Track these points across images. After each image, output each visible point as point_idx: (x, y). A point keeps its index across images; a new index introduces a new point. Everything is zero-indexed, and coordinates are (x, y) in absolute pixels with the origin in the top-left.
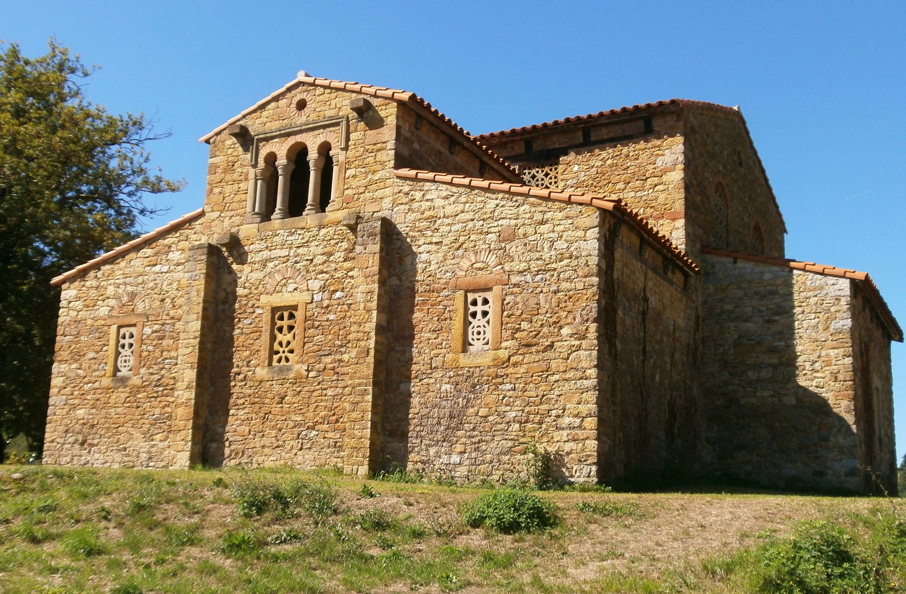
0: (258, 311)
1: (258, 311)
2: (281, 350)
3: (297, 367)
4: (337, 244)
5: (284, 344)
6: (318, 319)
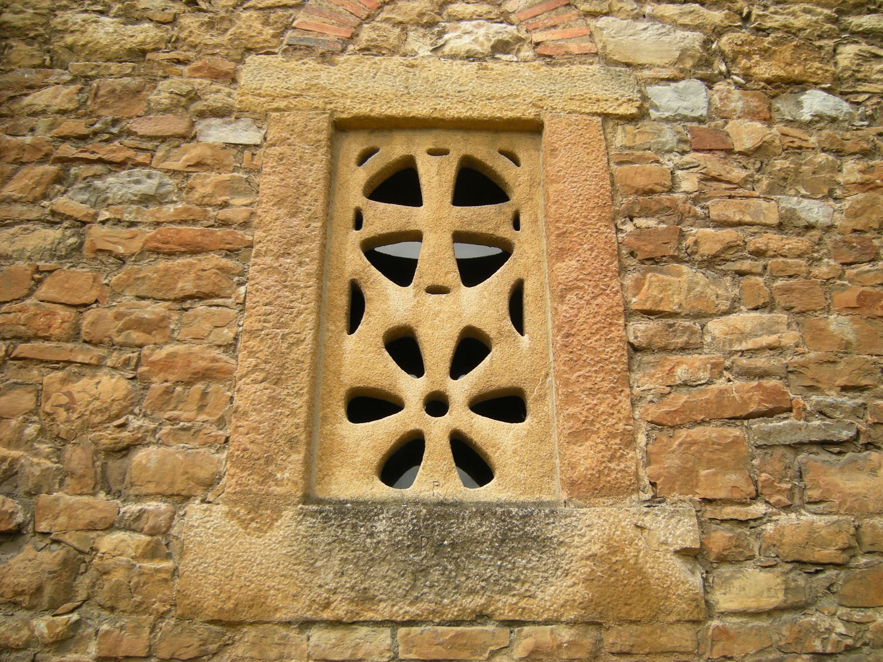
2: (412, 389)
3: (593, 527)
5: (438, 349)
6: (718, 209)
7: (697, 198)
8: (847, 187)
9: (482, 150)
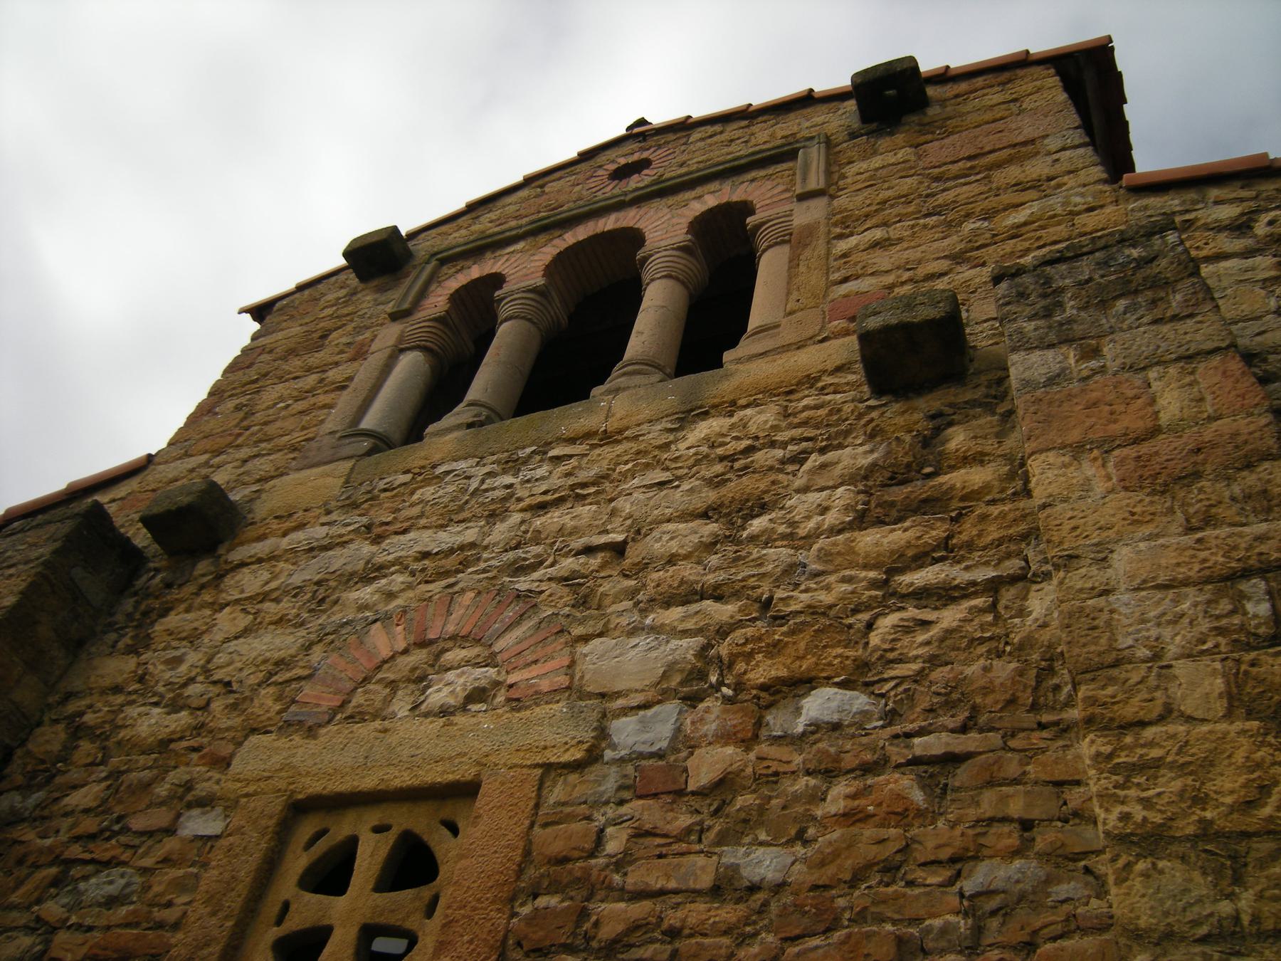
0: (199, 824)
1: (199, 824)
4: (799, 459)
7: (621, 863)
8: (823, 824)
9: (418, 820)
